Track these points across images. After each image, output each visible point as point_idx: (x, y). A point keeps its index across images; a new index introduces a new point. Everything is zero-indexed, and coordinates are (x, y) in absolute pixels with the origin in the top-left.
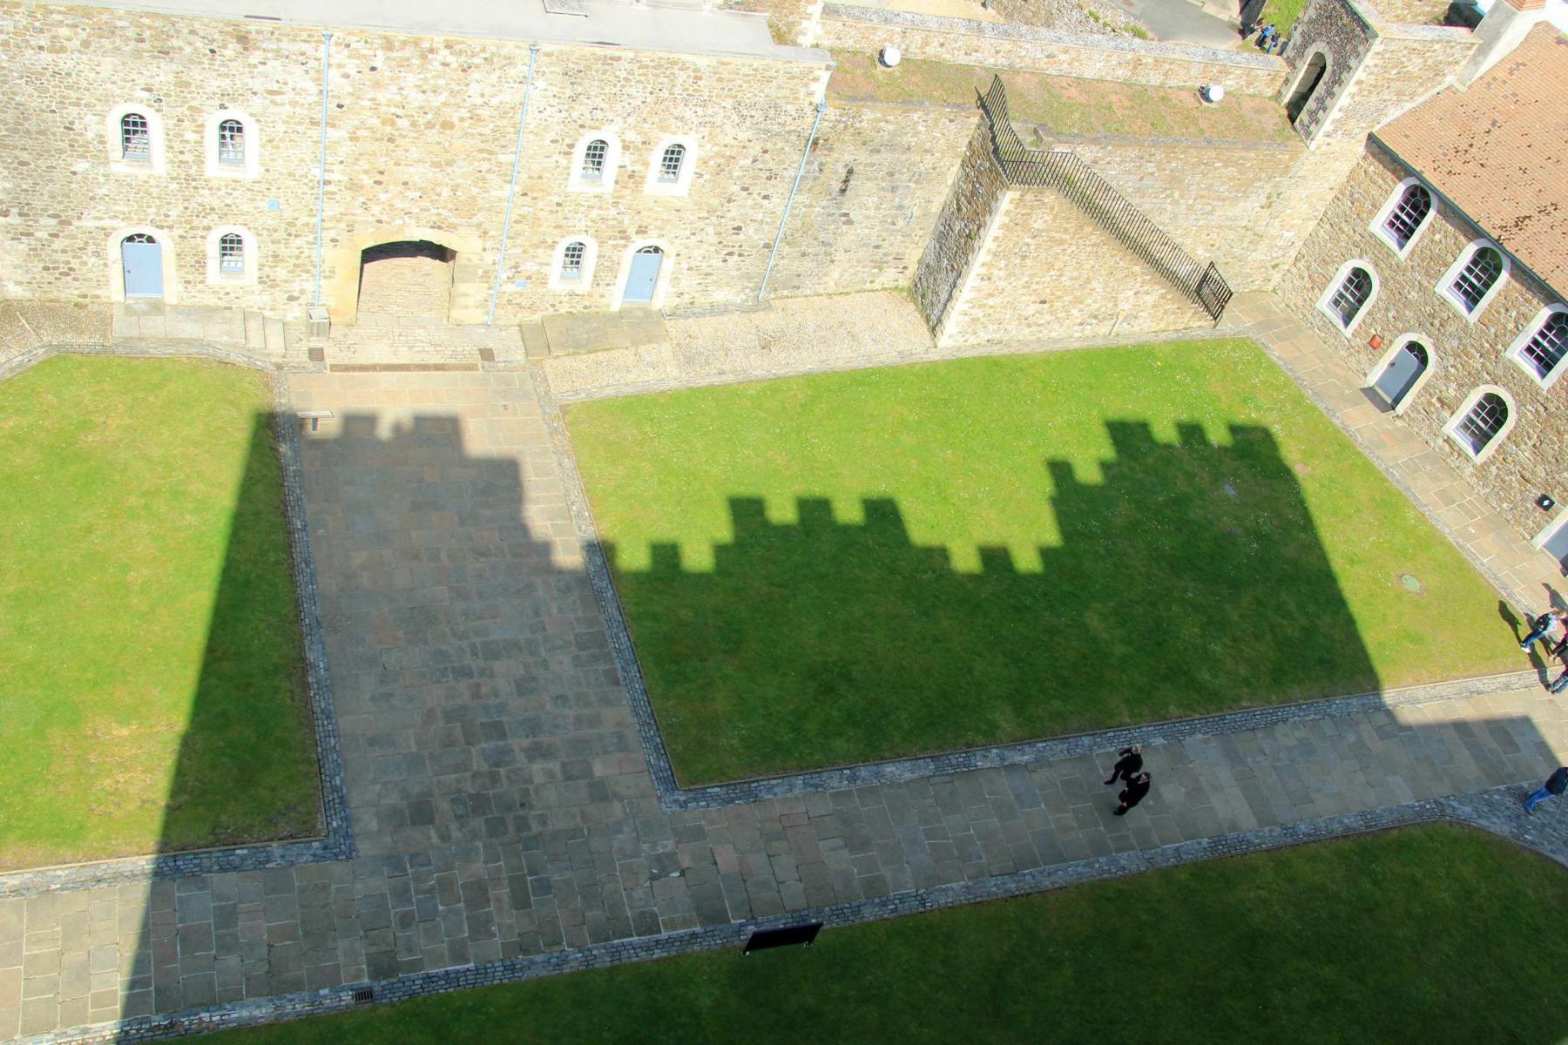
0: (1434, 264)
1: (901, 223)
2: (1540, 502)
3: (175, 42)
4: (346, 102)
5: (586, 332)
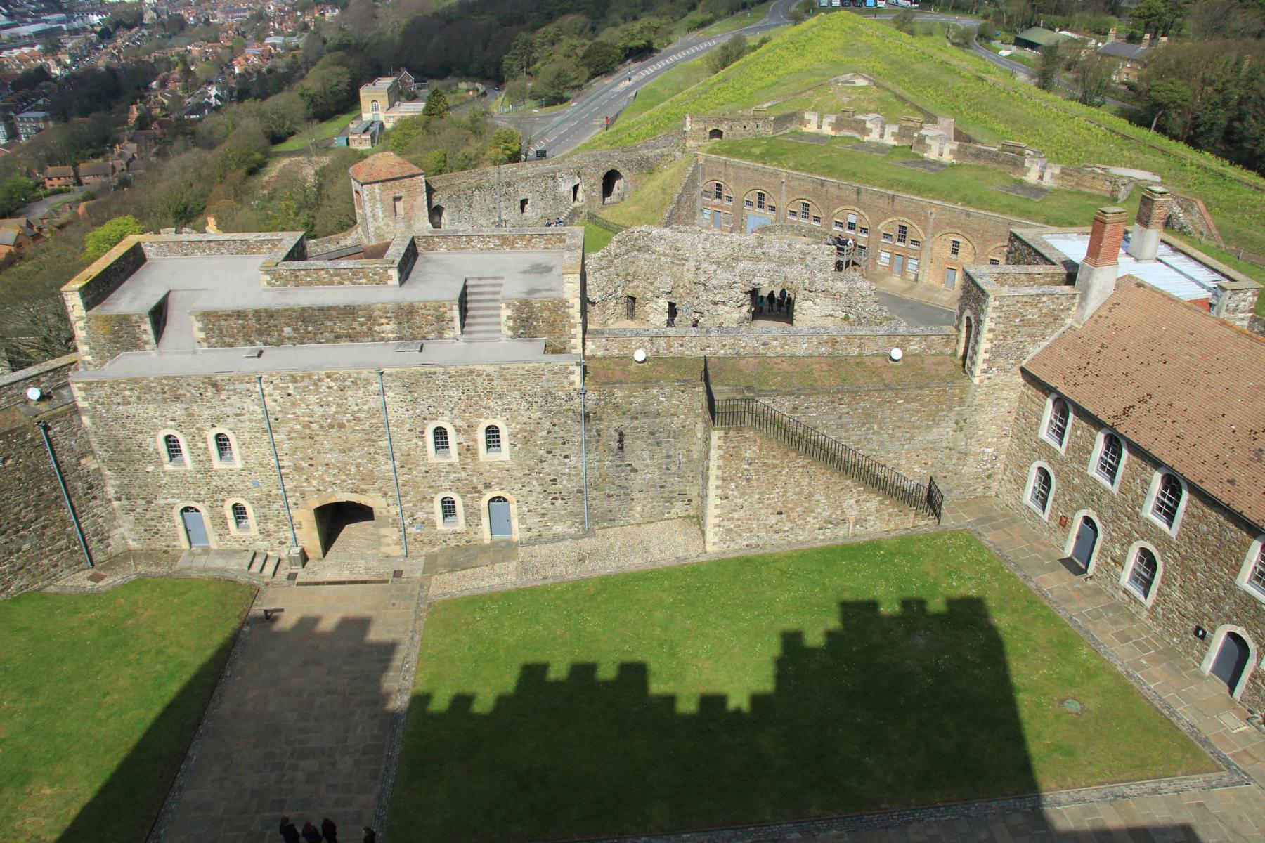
0: (1082, 453)
1: (674, 469)
2: (1196, 633)
3: (181, 392)
4: (280, 416)
5: (464, 556)
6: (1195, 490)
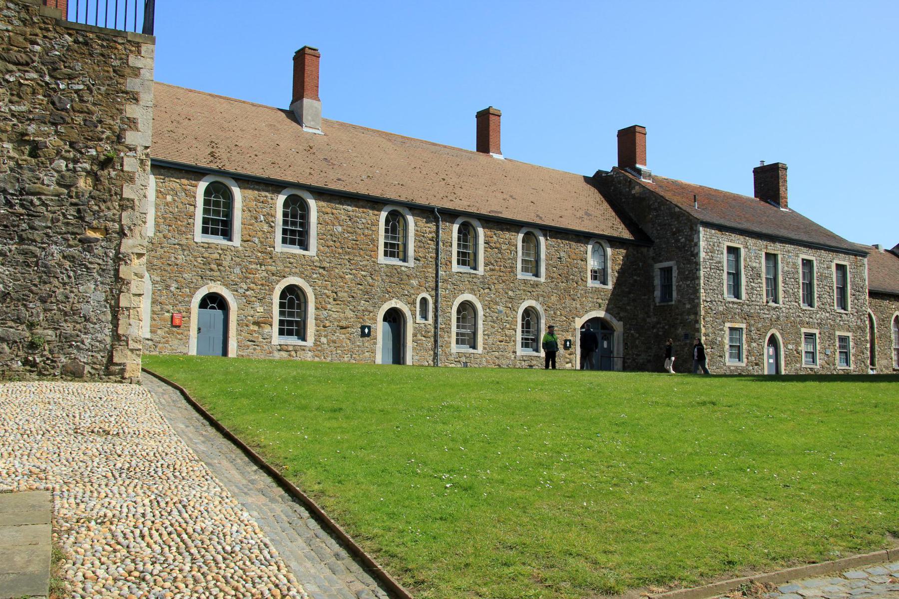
2: (363, 335)
6: (321, 193)
